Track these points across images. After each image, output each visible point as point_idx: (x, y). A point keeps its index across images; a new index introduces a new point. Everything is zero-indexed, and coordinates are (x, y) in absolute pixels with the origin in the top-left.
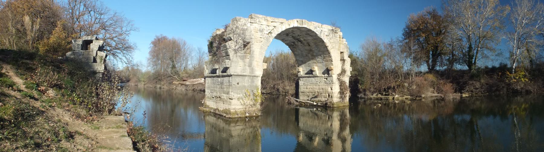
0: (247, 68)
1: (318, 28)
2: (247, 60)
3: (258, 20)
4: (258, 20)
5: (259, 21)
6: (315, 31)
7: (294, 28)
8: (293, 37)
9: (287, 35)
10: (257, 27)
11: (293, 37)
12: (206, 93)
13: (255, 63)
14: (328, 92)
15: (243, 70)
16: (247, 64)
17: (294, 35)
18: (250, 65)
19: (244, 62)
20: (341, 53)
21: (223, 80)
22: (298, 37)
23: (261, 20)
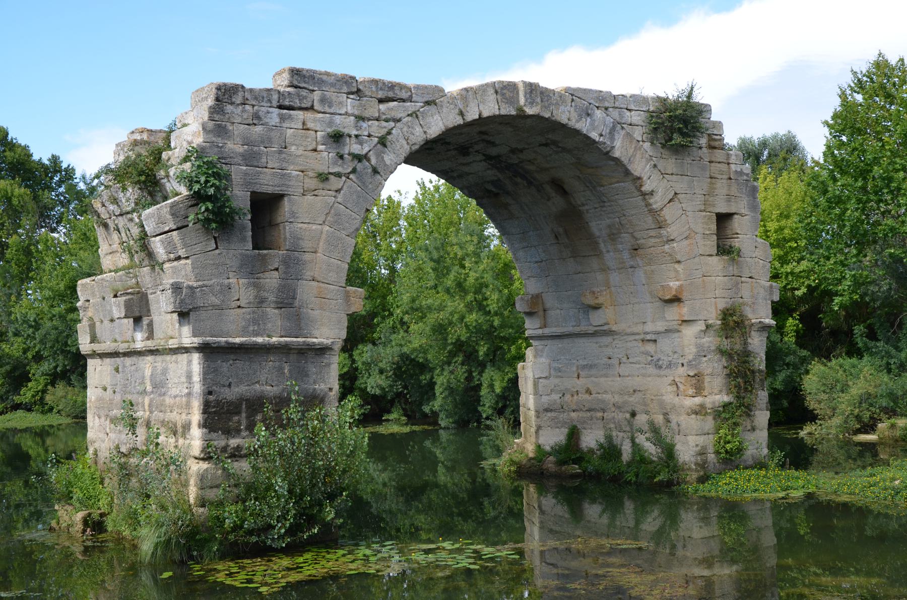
0: (272, 312)
1: (599, 113)
2: (272, 280)
3: (317, 96)
4: (317, 96)
5: (323, 100)
6: (583, 126)
7: (481, 121)
8: (488, 158)
9: (464, 150)
10: (310, 125)
11: (488, 158)
12: (90, 434)
13: (307, 291)
14: (662, 404)
15: (255, 322)
16: (272, 298)
17: (494, 151)
18: (287, 301)
19: (257, 286)
20: (723, 219)
21: (165, 371)
22: (514, 160)
23: (331, 94)
